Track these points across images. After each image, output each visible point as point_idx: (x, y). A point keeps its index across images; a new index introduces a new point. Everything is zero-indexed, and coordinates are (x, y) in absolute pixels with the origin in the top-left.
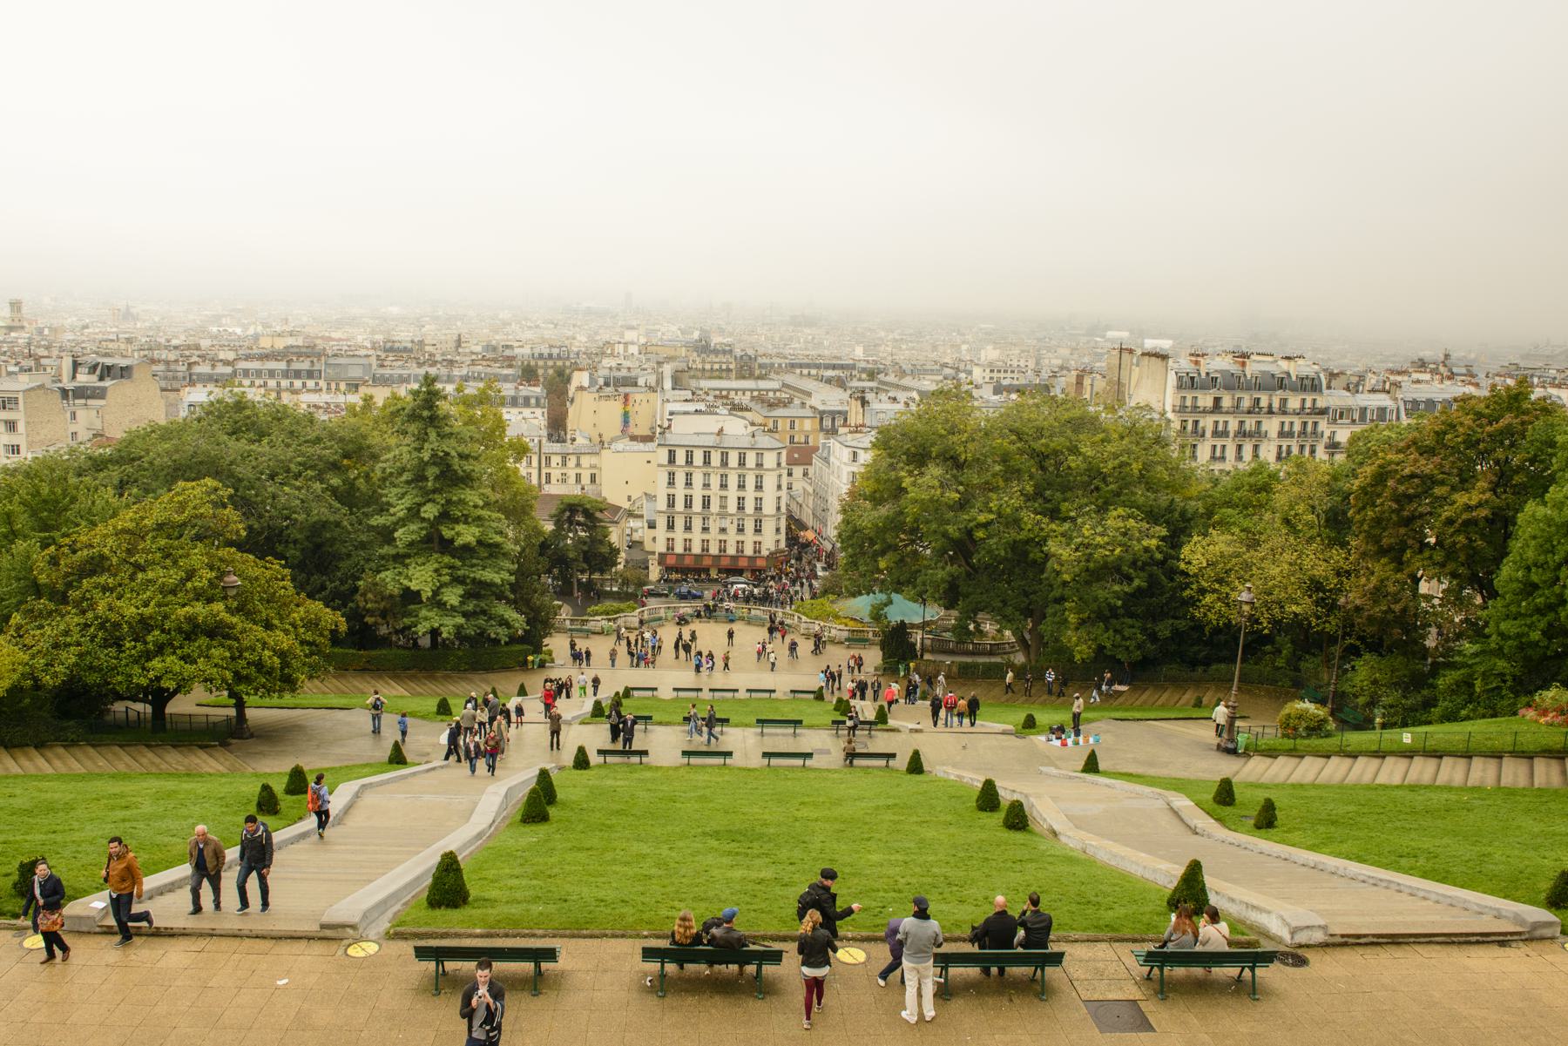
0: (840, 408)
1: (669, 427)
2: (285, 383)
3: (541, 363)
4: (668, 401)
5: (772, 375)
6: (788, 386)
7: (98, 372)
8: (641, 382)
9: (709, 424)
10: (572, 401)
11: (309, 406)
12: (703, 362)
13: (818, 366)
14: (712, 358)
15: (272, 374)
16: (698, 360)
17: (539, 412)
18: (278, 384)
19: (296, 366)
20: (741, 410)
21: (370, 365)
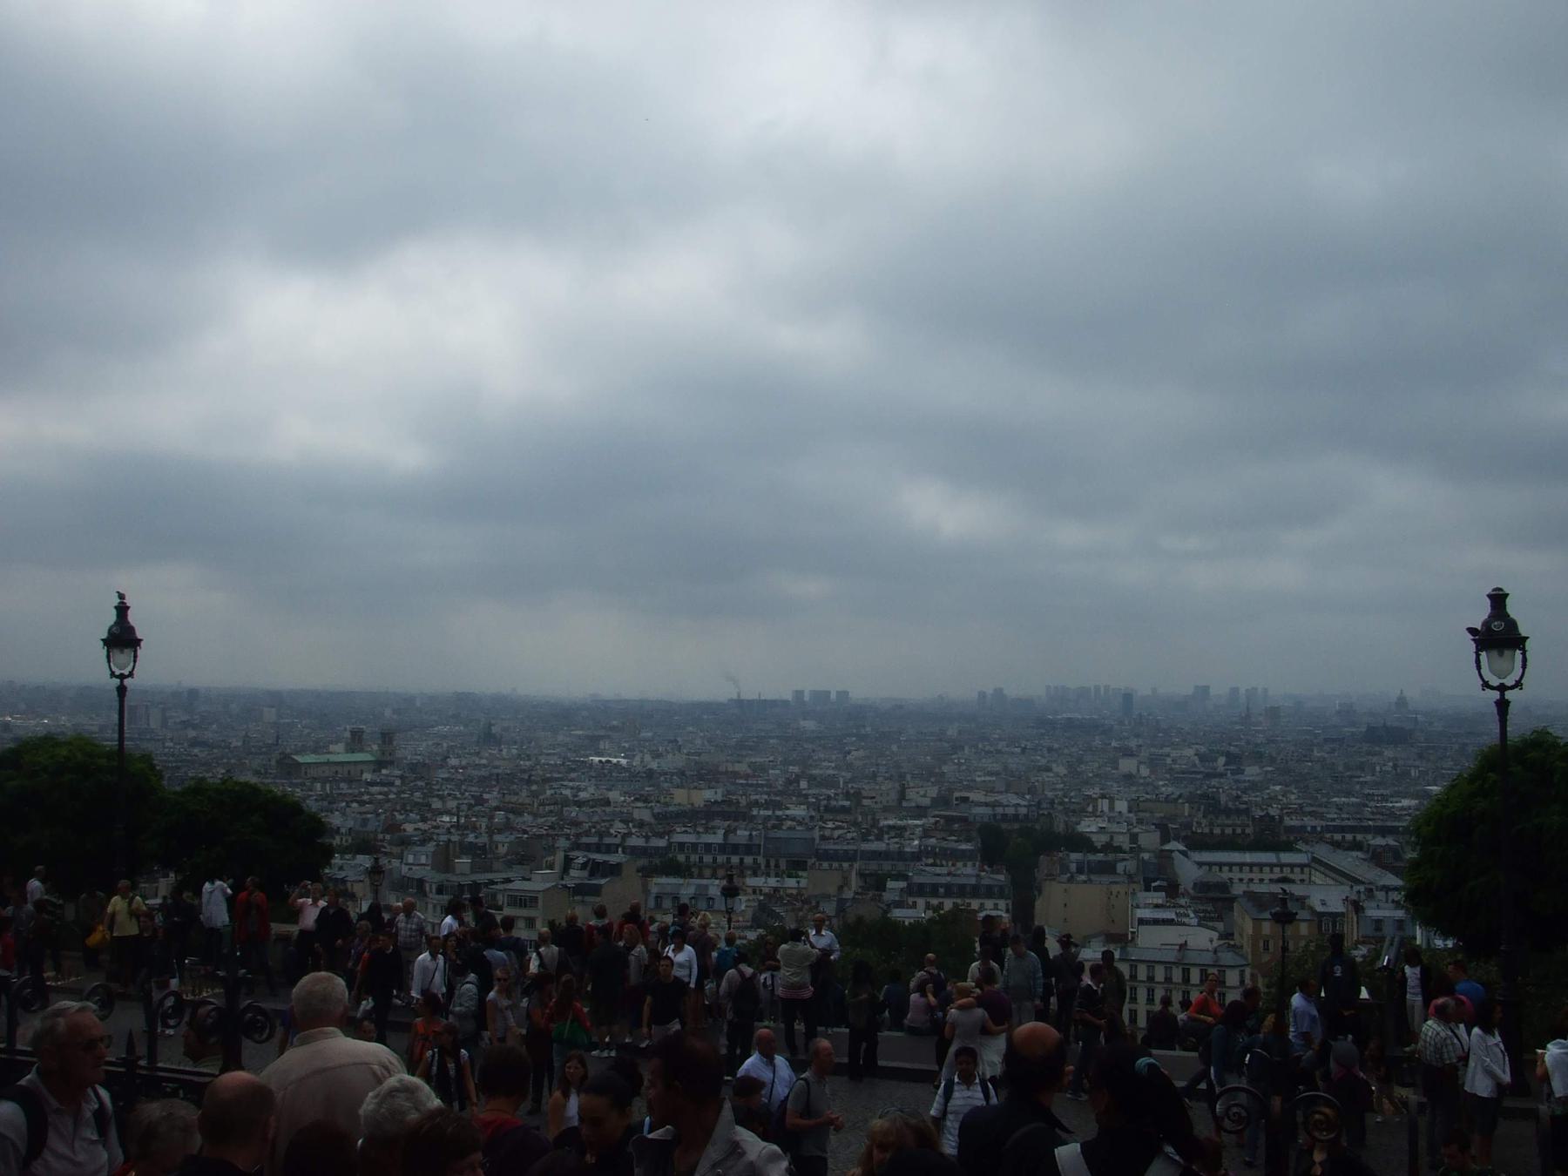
0: (1341, 909)
1: (1133, 938)
2: (721, 859)
3: (1004, 826)
4: (1138, 907)
5: (1300, 845)
6: (1320, 862)
7: (588, 868)
8: (1120, 867)
9: (1172, 935)
10: (1040, 892)
11: (754, 892)
12: (1211, 824)
13: (1367, 830)
14: (1222, 820)
15: (708, 847)
16: (1204, 822)
17: (1002, 904)
18: (715, 860)
19: (733, 839)
20: (1212, 919)
21: (813, 839)
